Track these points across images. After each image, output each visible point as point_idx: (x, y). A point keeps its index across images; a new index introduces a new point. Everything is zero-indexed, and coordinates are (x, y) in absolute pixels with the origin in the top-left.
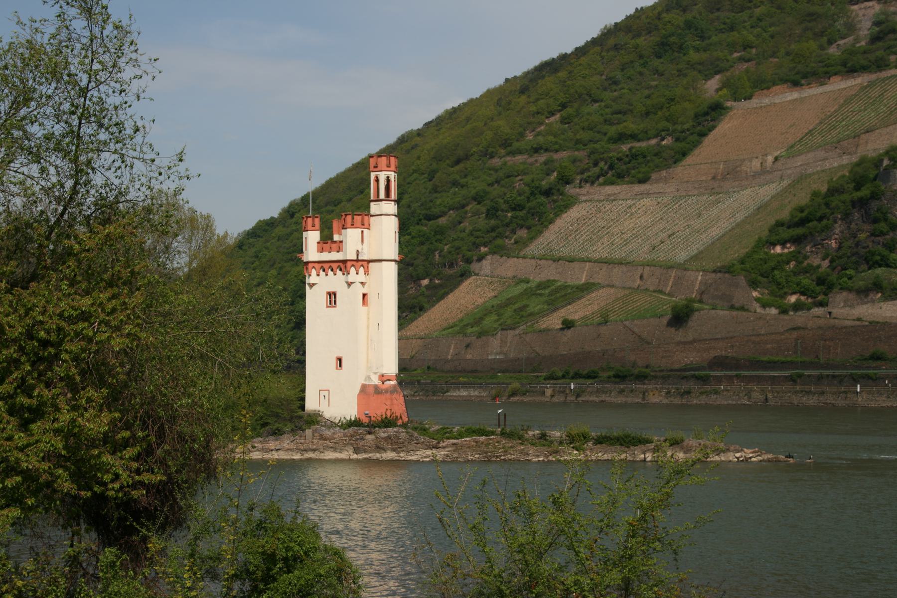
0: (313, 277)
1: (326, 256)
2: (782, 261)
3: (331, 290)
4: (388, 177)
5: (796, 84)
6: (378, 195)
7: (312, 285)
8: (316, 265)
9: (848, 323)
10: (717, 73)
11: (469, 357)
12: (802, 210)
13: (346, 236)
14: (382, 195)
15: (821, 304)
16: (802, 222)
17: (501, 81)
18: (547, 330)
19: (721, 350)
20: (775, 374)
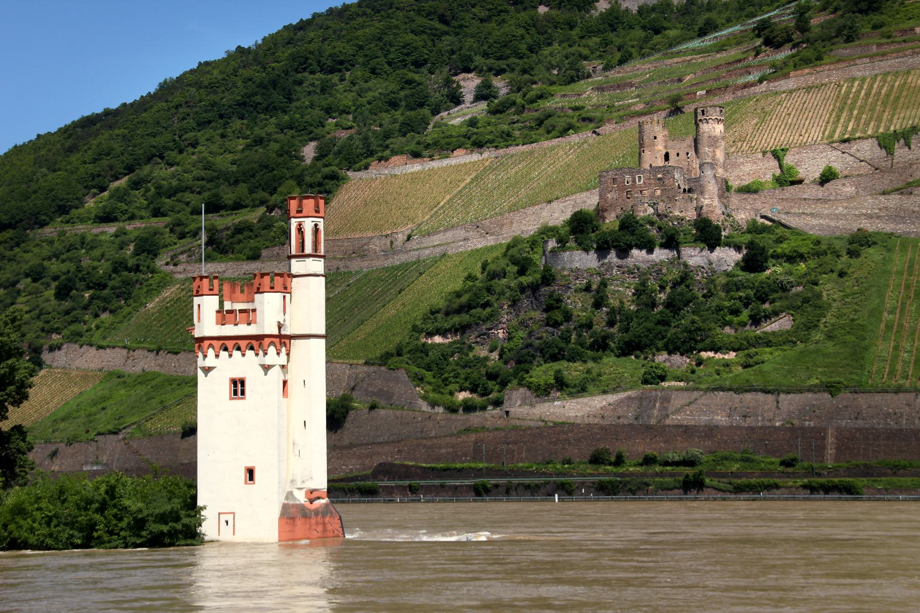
1: (229, 330)
2: (445, 354)
3: (237, 375)
4: (316, 225)
5: (416, 155)
6: (303, 251)
7: (207, 370)
8: (214, 342)
9: (532, 424)
10: (312, 140)
11: (56, 468)
12: (458, 295)
13: (262, 303)
14: (308, 249)
15: (498, 403)
16: (466, 308)
17: (34, 137)
18: (160, 435)
19: (387, 456)
20: (458, 483)
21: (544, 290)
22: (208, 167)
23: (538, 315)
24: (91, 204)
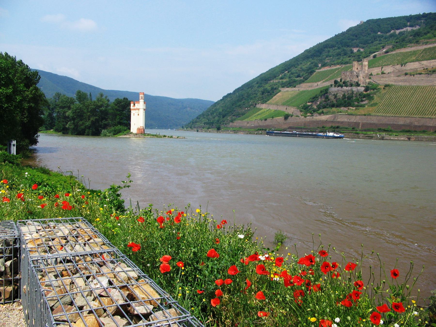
0: (132, 111)
2: (309, 106)
11: (248, 125)
21: (326, 95)
22: (301, 68)
23: (324, 100)
24: (281, 76)
